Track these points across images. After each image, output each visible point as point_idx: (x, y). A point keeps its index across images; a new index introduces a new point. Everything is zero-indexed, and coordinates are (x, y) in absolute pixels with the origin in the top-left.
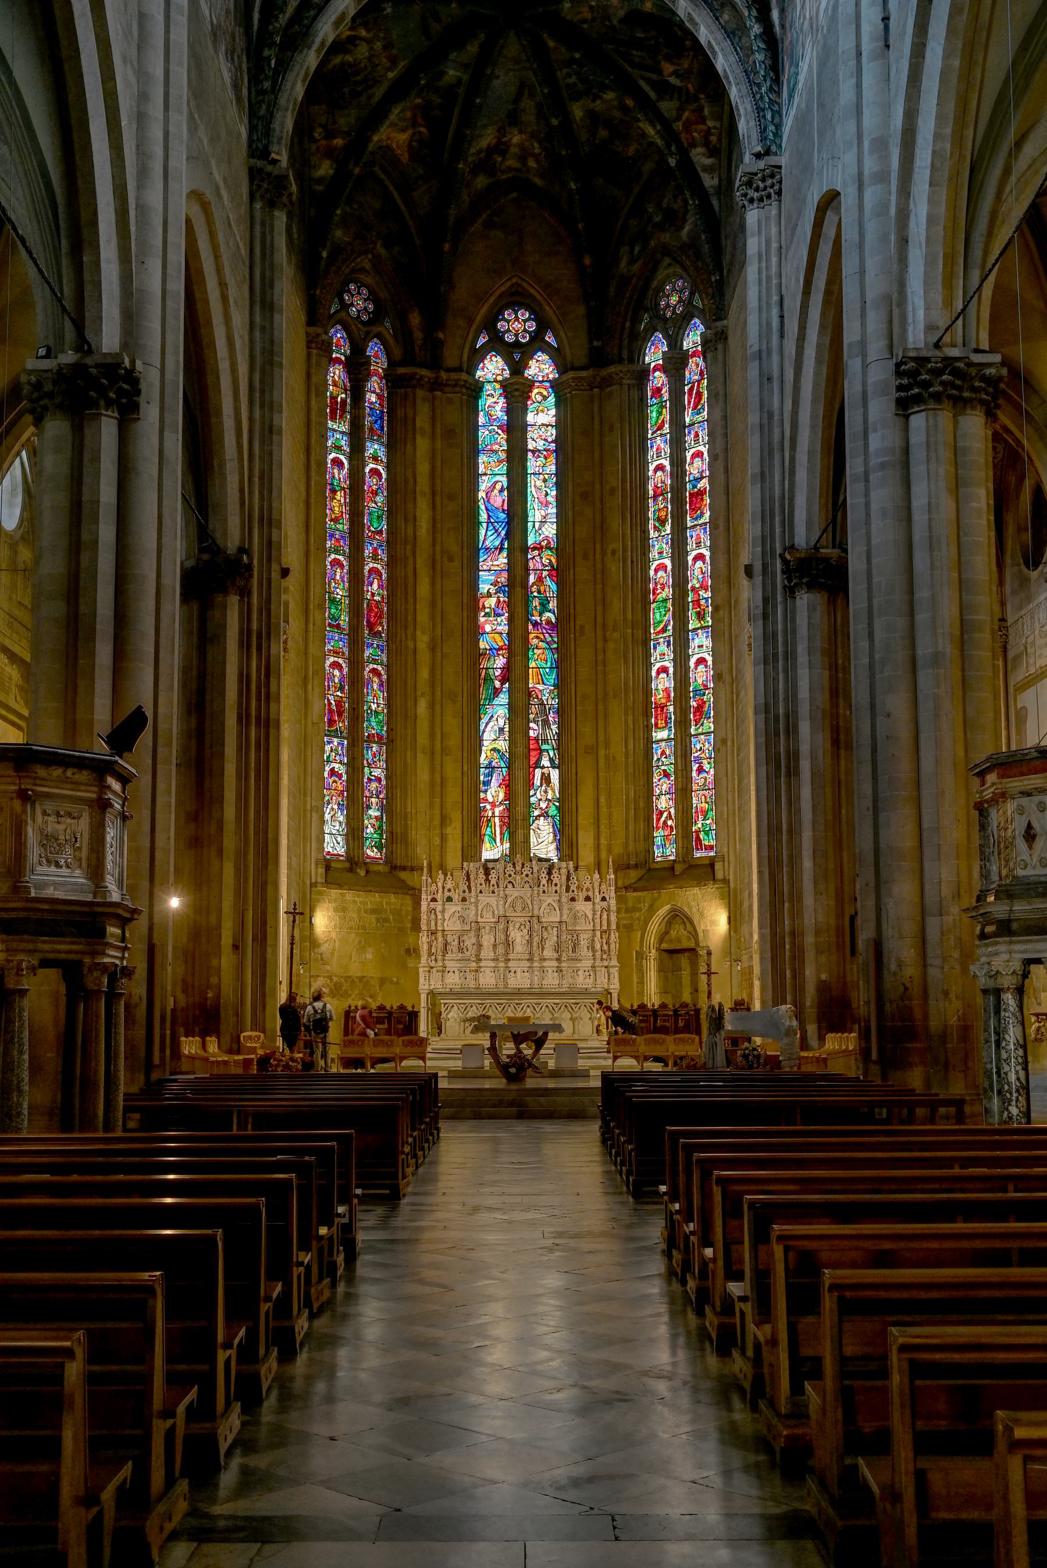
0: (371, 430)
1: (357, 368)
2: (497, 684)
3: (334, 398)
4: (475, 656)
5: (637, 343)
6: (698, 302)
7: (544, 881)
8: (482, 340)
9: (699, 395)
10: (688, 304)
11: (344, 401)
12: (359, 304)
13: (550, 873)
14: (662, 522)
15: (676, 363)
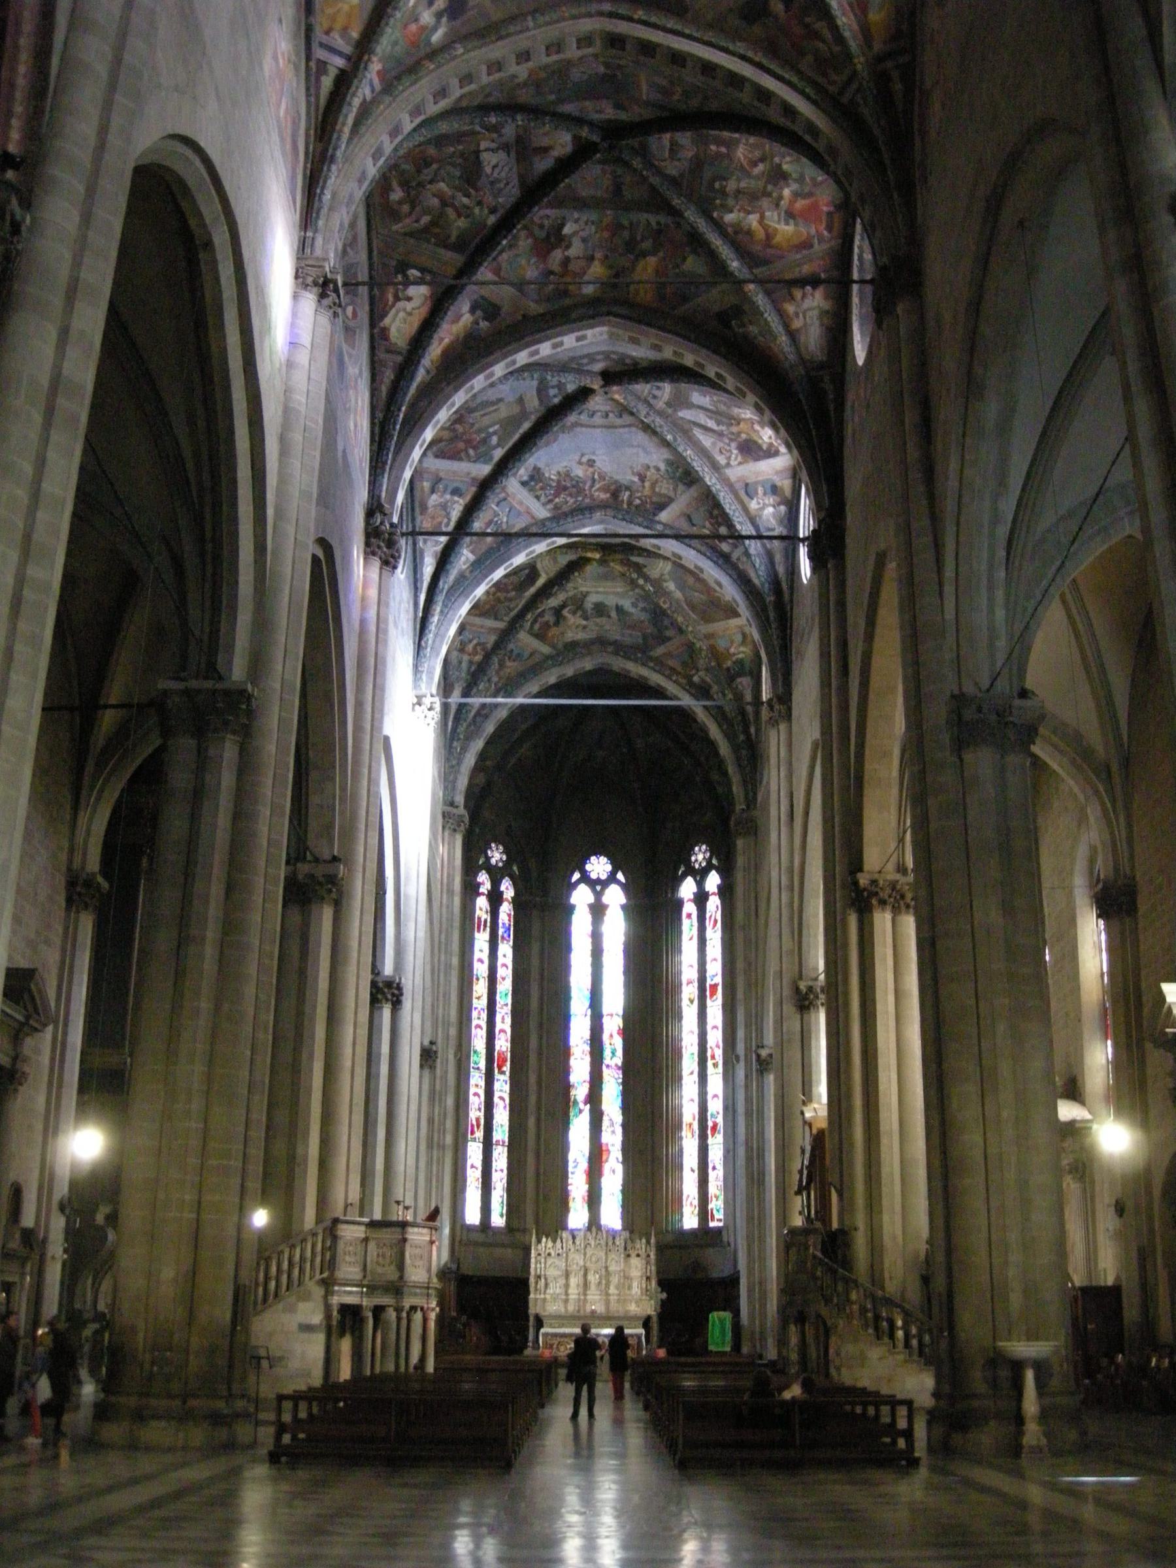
0: (503, 938)
1: (495, 898)
2: (581, 1106)
3: (479, 919)
4: (567, 1087)
5: (678, 881)
6: (714, 862)
7: (610, 1243)
8: (576, 876)
9: (716, 921)
10: (709, 861)
11: (486, 921)
12: (497, 856)
13: (614, 1238)
14: (692, 1001)
15: (701, 899)
